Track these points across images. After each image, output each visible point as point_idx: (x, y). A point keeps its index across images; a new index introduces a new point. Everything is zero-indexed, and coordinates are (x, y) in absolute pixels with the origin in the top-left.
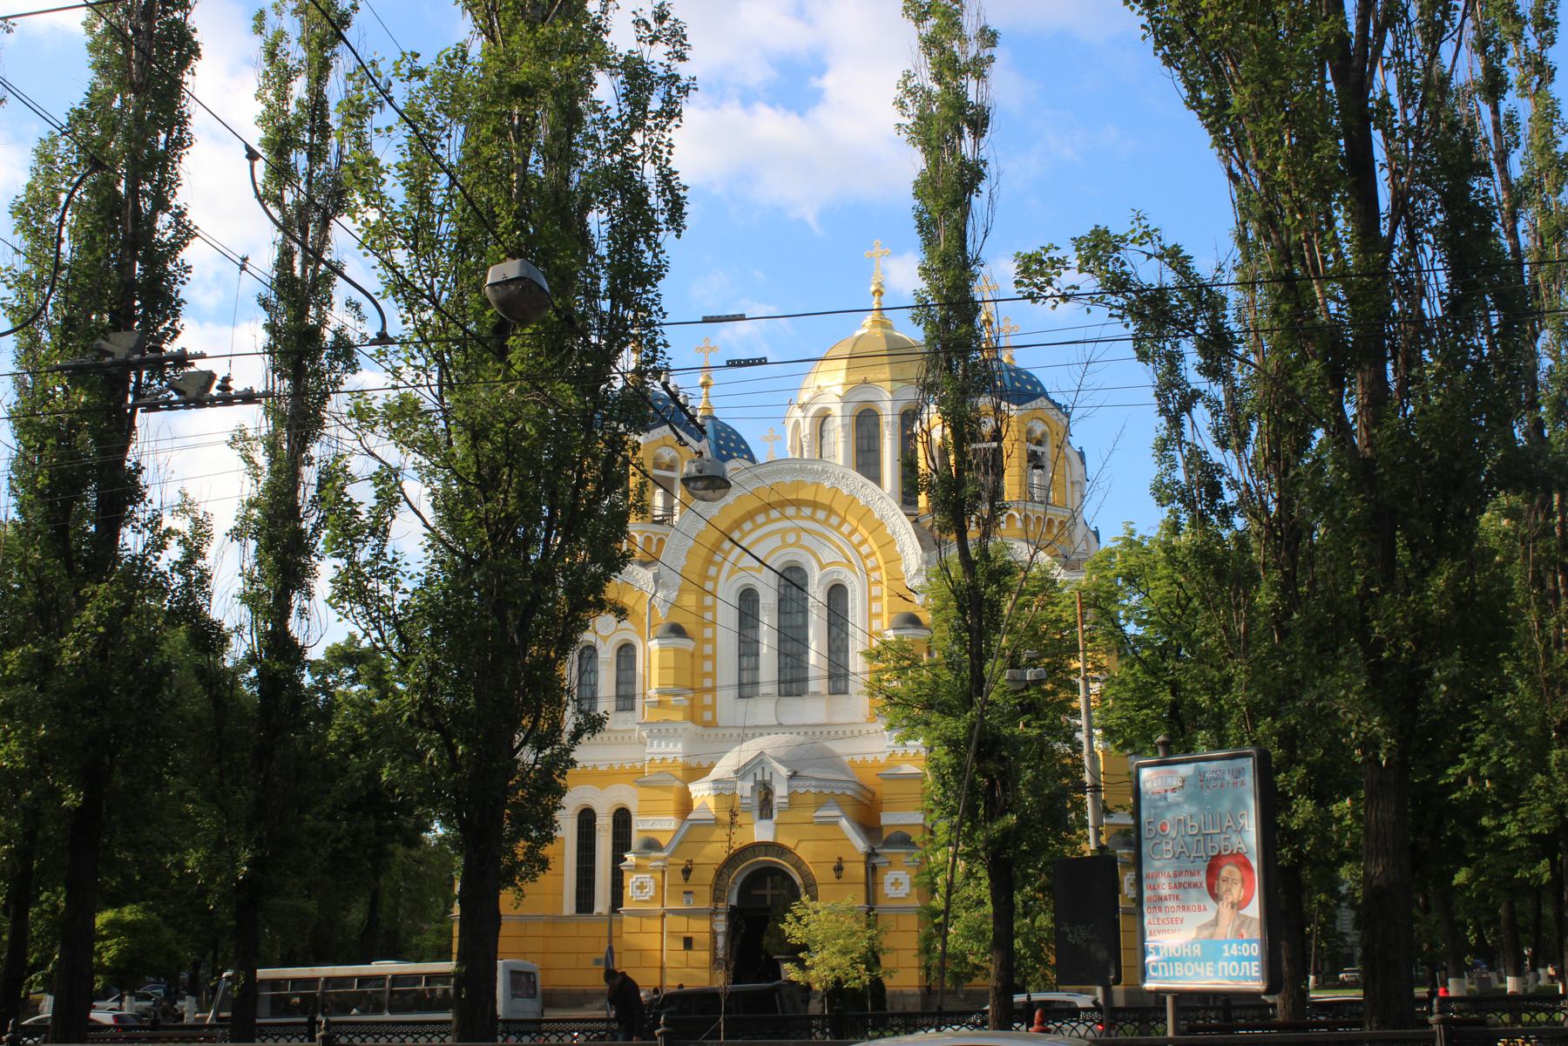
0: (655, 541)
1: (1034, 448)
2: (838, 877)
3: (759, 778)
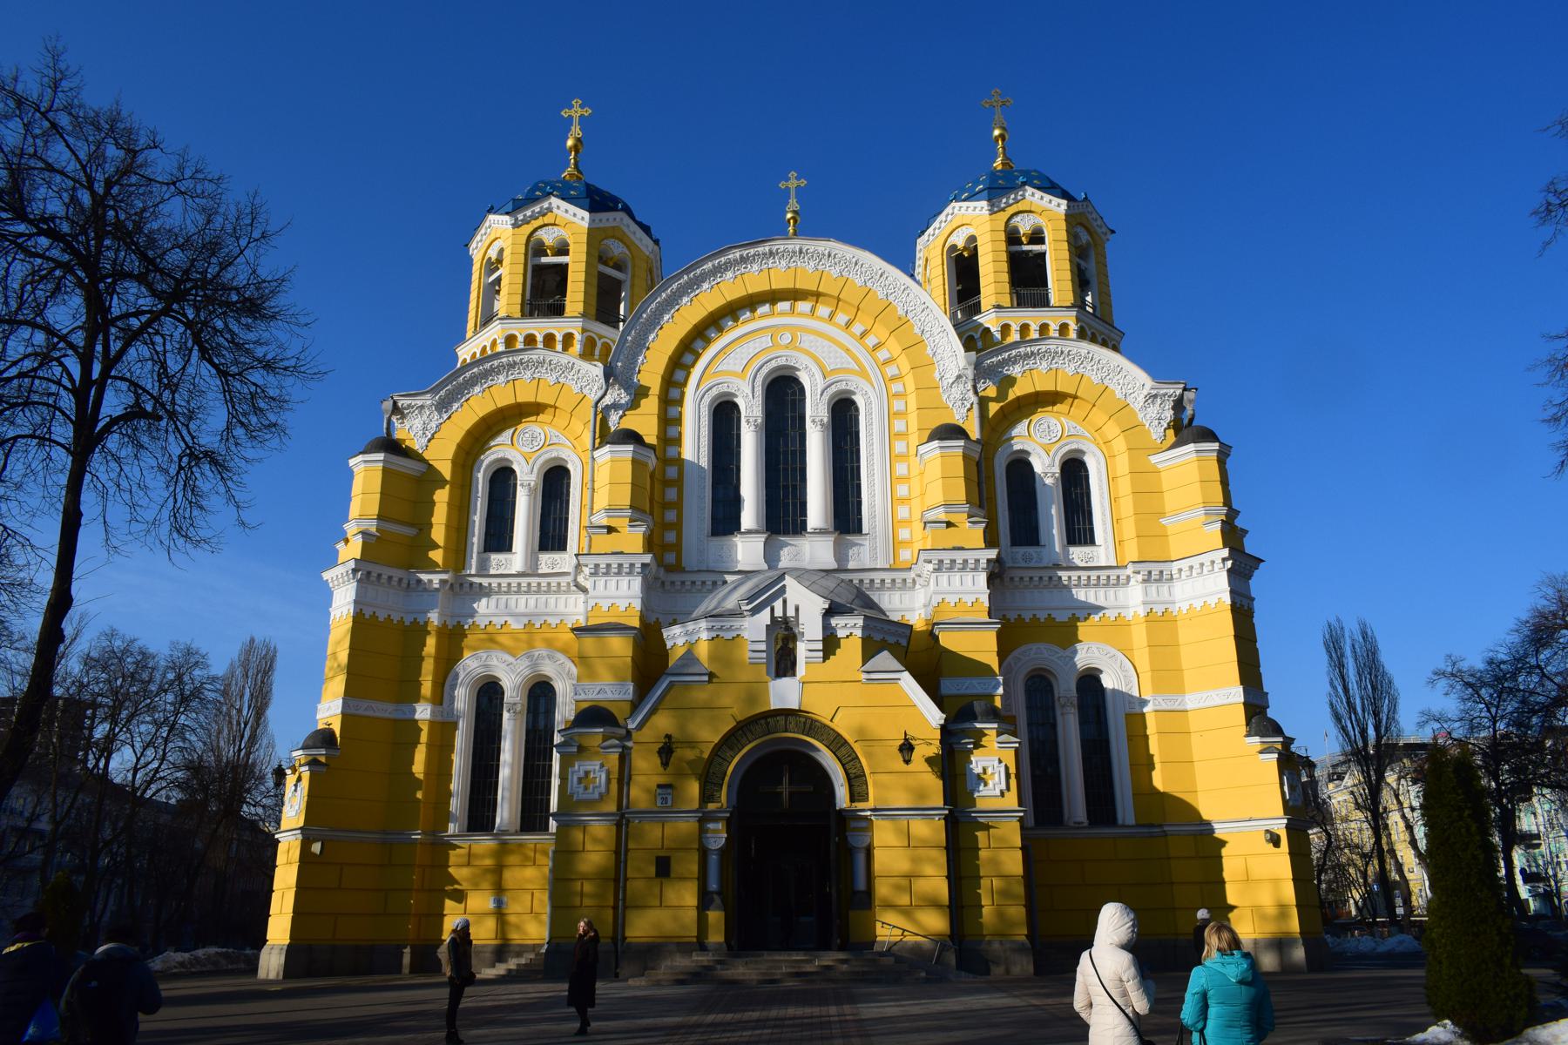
0: (599, 344)
1: (1078, 260)
2: (907, 762)
3: (779, 613)
